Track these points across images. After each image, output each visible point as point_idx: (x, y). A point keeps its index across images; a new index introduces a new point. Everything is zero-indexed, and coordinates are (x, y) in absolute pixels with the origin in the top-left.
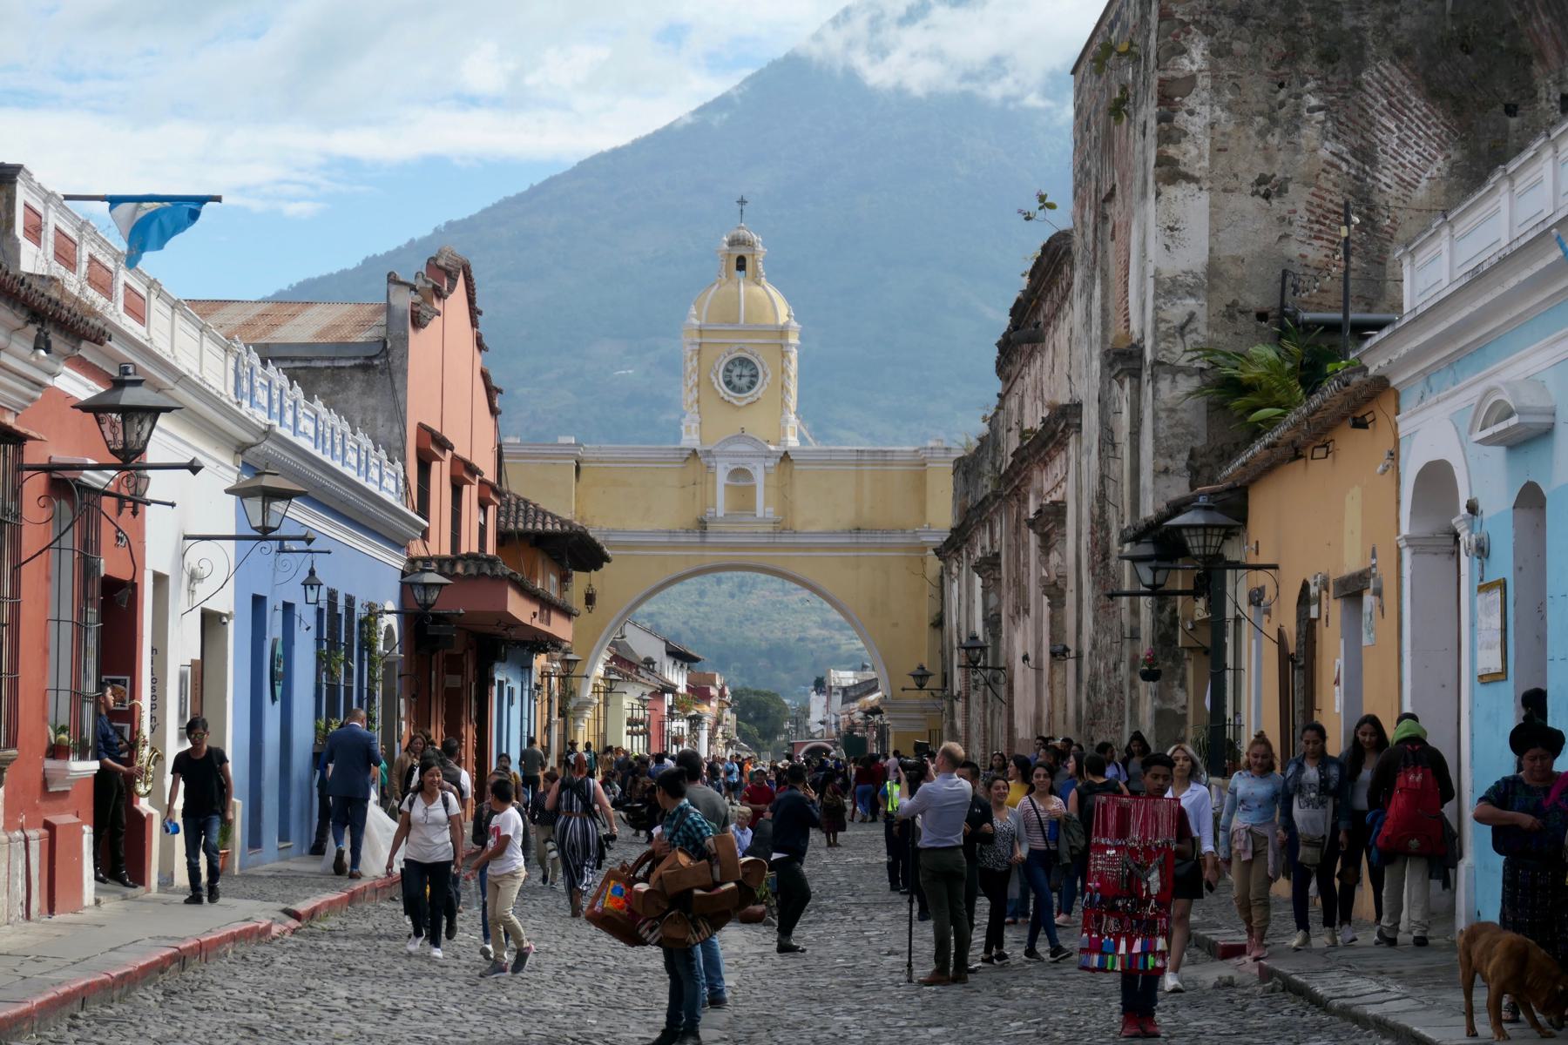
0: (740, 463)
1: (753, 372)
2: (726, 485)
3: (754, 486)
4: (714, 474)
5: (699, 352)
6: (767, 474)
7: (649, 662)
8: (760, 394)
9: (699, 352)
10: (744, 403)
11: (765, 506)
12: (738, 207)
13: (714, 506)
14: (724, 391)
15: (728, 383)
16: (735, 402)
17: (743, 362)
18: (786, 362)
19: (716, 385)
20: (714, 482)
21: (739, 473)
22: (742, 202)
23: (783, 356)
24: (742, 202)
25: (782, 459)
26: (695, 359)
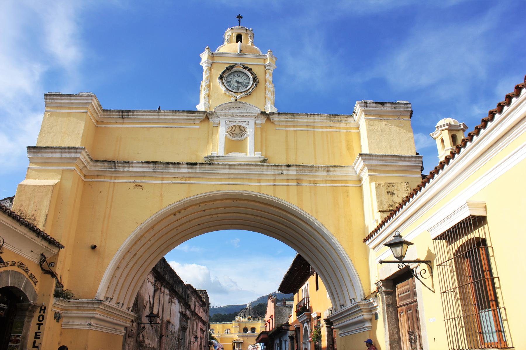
11: (256, 150)
22: (239, 17)
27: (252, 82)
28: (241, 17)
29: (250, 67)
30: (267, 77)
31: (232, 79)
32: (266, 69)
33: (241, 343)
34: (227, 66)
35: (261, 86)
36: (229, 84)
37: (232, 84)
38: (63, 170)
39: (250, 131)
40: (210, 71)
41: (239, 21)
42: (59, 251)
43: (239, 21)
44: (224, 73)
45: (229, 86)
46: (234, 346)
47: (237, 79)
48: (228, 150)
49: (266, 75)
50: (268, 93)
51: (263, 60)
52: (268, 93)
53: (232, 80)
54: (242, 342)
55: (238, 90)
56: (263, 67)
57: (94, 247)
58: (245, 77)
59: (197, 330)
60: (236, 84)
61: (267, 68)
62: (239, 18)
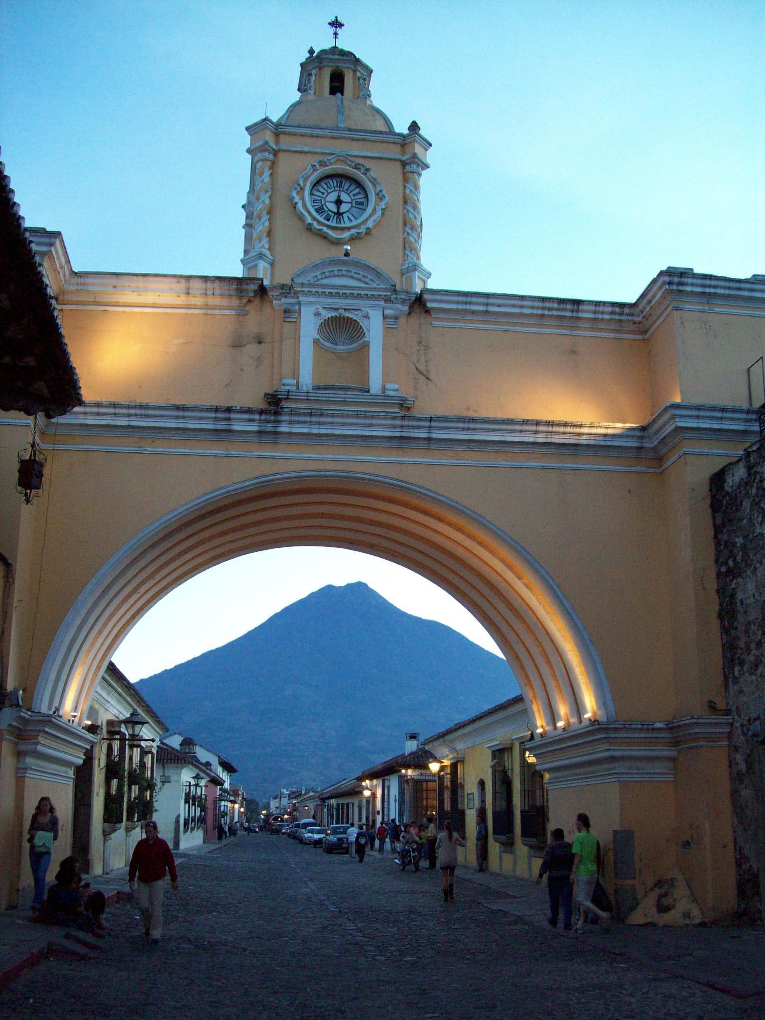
2: (316, 342)
3: (366, 346)
4: (297, 324)
6: (387, 329)
7: (208, 764)
8: (370, 224)
10: (346, 235)
12: (332, 30)
13: (296, 375)
15: (320, 210)
16: (331, 233)
18: (410, 186)
19: (300, 206)
20: (297, 339)
22: (336, 24)
23: (406, 180)
24: (336, 24)
25: (411, 307)
26: (267, 173)
28: (341, 25)
29: (368, 164)
30: (408, 191)
31: (323, 193)
32: (406, 170)
37: (324, 206)
40: (270, 172)
41: (336, 34)
43: (336, 34)
45: (317, 211)
49: (405, 187)
50: (410, 232)
51: (397, 148)
52: (410, 232)
53: (324, 196)
56: (398, 165)
61: (408, 167)
62: (336, 27)
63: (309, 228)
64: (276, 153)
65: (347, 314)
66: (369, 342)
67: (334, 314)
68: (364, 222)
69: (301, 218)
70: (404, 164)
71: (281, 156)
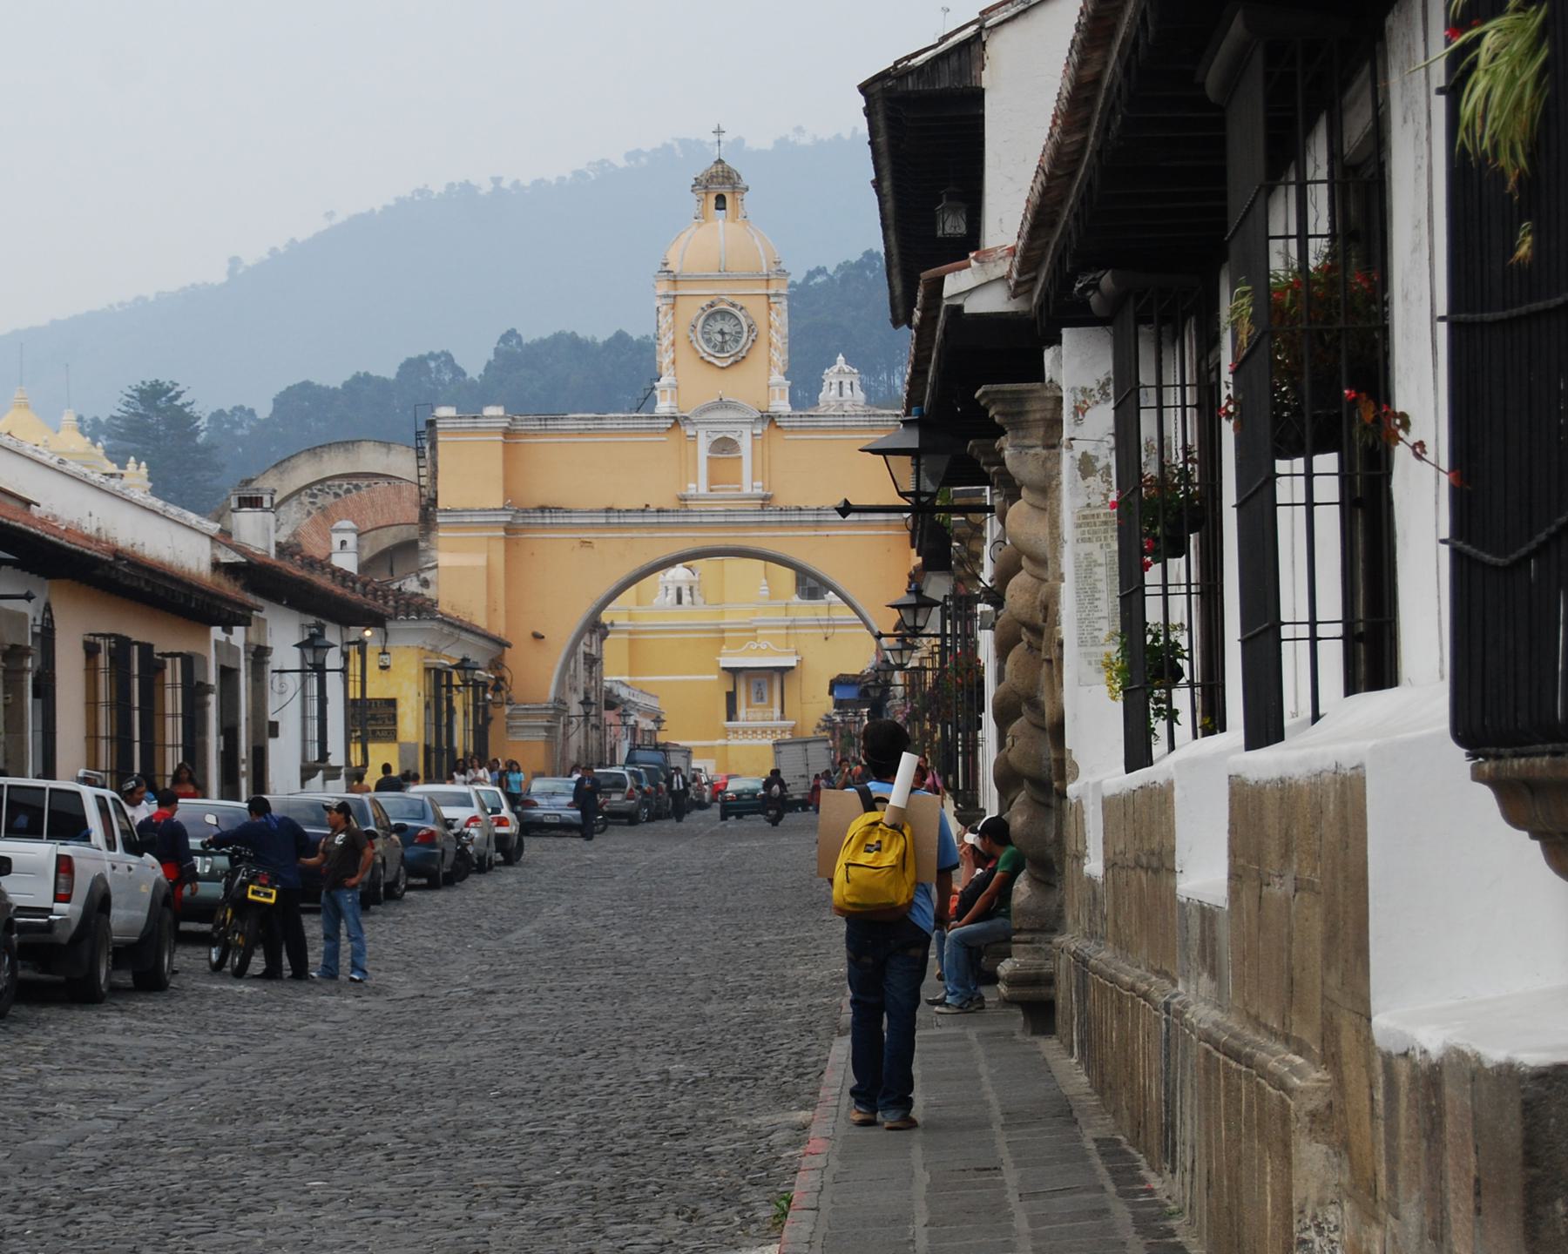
0: (727, 431)
1: (738, 328)
4: (695, 442)
5: (674, 306)
9: (674, 306)
11: (753, 480)
12: (715, 138)
13: (696, 482)
14: (704, 349)
15: (708, 341)
17: (724, 314)
18: (773, 314)
21: (724, 446)
26: (670, 315)
27: (745, 335)
29: (738, 301)
33: (783, 671)
34: (704, 302)
35: (762, 344)
36: (706, 336)
38: (489, 538)
39: (745, 444)
42: (503, 651)
44: (698, 318)
46: (731, 698)
47: (718, 327)
48: (712, 480)
51: (764, 283)
54: (792, 668)
55: (722, 350)
56: (765, 298)
57: (537, 637)
58: (733, 322)
59: (575, 670)
60: (719, 338)
61: (772, 300)
63: (702, 358)
64: (675, 296)
65: (729, 436)
66: (740, 457)
67: (720, 436)
68: (740, 351)
69: (697, 352)
70: (768, 296)
71: (678, 298)
